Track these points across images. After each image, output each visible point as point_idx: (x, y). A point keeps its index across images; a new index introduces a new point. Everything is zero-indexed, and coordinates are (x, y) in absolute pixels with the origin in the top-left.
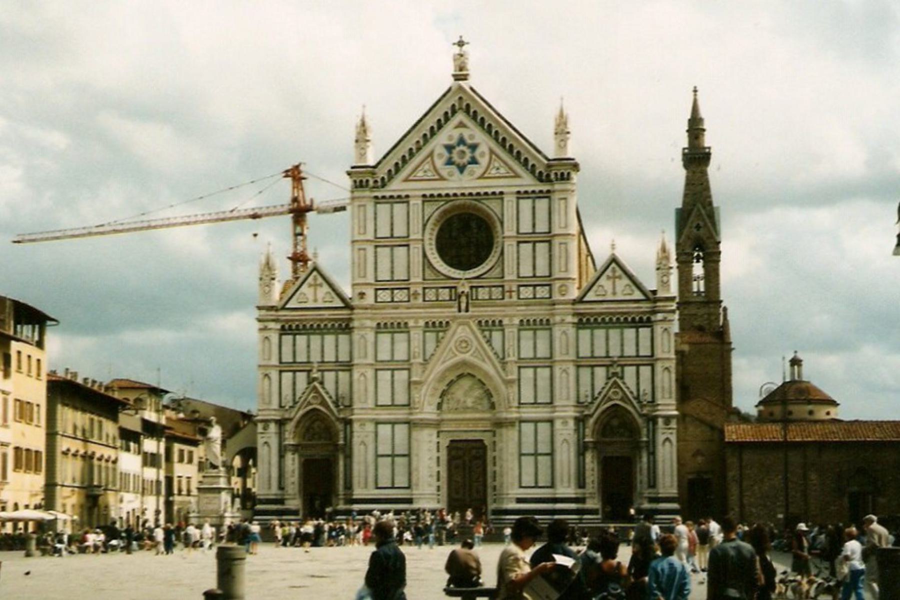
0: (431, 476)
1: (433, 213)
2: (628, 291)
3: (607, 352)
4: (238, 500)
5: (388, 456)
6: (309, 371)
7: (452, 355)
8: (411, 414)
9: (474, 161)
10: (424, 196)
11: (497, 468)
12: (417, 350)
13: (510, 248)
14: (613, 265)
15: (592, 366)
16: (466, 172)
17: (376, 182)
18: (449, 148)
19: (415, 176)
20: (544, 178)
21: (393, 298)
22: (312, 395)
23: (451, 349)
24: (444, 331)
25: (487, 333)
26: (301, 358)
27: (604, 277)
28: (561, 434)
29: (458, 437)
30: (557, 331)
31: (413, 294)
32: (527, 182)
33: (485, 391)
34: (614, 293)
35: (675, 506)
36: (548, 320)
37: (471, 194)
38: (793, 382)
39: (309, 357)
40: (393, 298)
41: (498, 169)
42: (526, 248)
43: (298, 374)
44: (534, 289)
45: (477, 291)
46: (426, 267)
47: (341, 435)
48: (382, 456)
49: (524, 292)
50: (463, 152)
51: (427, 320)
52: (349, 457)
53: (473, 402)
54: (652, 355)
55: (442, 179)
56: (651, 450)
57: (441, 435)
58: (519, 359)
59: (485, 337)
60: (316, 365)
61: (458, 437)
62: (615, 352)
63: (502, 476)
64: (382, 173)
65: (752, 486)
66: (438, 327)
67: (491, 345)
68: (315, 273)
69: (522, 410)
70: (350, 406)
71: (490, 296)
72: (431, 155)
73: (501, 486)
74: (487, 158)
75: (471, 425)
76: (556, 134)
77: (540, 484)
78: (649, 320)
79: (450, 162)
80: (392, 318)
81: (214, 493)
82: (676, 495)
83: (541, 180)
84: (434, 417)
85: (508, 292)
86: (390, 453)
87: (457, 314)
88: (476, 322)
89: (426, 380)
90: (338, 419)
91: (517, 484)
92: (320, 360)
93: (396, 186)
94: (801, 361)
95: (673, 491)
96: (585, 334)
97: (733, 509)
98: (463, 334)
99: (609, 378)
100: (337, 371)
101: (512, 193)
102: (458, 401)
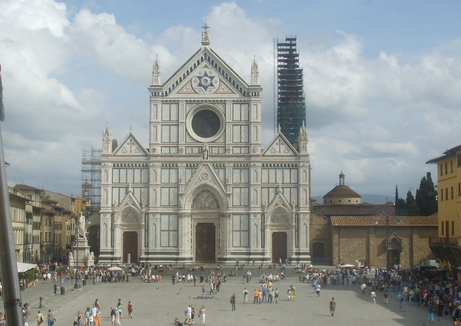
0: (188, 241)
1: (191, 109)
2: (286, 151)
3: (276, 181)
4: (93, 253)
6: (127, 188)
8: (179, 210)
10: (187, 101)
11: (221, 238)
12: (182, 178)
13: (229, 128)
15: (269, 188)
16: (208, 89)
17: (163, 93)
18: (200, 78)
20: (246, 94)
21: (170, 152)
24: (196, 169)
25: (217, 170)
26: (123, 180)
27: (275, 143)
30: (252, 171)
31: (180, 150)
32: (237, 96)
33: (215, 199)
34: (280, 152)
35: (308, 256)
36: (247, 164)
37: (210, 101)
38: (340, 185)
39: (127, 180)
40: (170, 152)
41: (223, 89)
42: (237, 128)
43: (121, 189)
44: (241, 149)
45: (212, 149)
46: (187, 135)
47: (143, 220)
49: (235, 150)
50: (206, 80)
51: (187, 163)
52: (147, 231)
53: (209, 205)
54: (298, 183)
55: (196, 93)
57: (192, 220)
58: (233, 183)
59: (216, 172)
60: (130, 184)
62: (279, 181)
63: (223, 241)
64: (166, 89)
65: (344, 247)
66: (192, 167)
68: (131, 138)
70: (148, 206)
71: (219, 152)
72: (191, 81)
73: (223, 245)
74: (218, 83)
75: (208, 216)
76: (252, 73)
78: (296, 165)
79: (200, 85)
81: (82, 250)
82: (309, 251)
83: (244, 95)
84: (190, 211)
85: (227, 150)
86: (168, 229)
87: (203, 160)
88: (212, 164)
89: (187, 193)
90: (142, 212)
91: (231, 246)
92: (133, 182)
93: (173, 96)
94: (344, 176)
95: (307, 250)
96: (265, 172)
97: (335, 258)
99: (276, 194)
102: (202, 204)
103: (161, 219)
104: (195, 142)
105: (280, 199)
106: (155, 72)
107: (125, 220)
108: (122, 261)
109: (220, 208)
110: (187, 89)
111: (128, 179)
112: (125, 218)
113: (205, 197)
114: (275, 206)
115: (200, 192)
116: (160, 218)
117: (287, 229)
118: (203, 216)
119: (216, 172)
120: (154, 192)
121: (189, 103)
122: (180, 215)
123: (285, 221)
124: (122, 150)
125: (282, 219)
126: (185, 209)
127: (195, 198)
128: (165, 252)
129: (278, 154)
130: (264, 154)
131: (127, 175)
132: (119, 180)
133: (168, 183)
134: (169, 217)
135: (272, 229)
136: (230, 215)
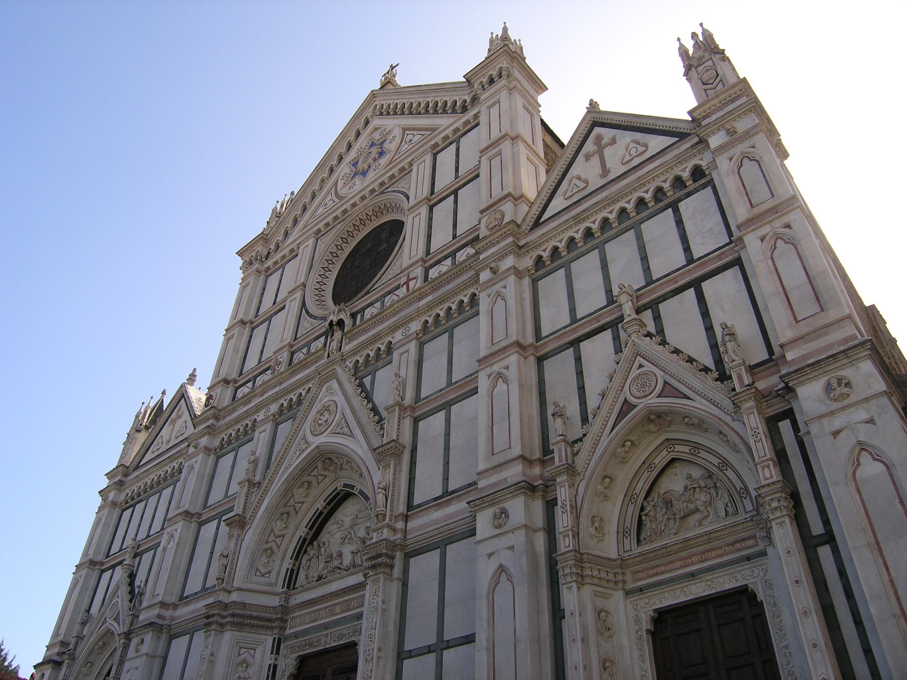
9: (381, 154)
10: (319, 231)
23: (304, 438)
27: (581, 157)
28: (490, 555)
32: (446, 123)
34: (605, 171)
56: (817, 528)
59: (361, 385)
67: (369, 398)
69: (411, 525)
72: (336, 184)
74: (398, 139)
75: (338, 609)
84: (275, 601)
88: (351, 365)
98: (327, 399)
103: (165, 659)
105: (641, 366)
114: (621, 415)
116: (160, 651)
117: (748, 558)
119: (361, 385)
125: (703, 497)
126: (236, 584)
127: (301, 537)
130: (540, 217)
135: (641, 590)
136: (393, 558)
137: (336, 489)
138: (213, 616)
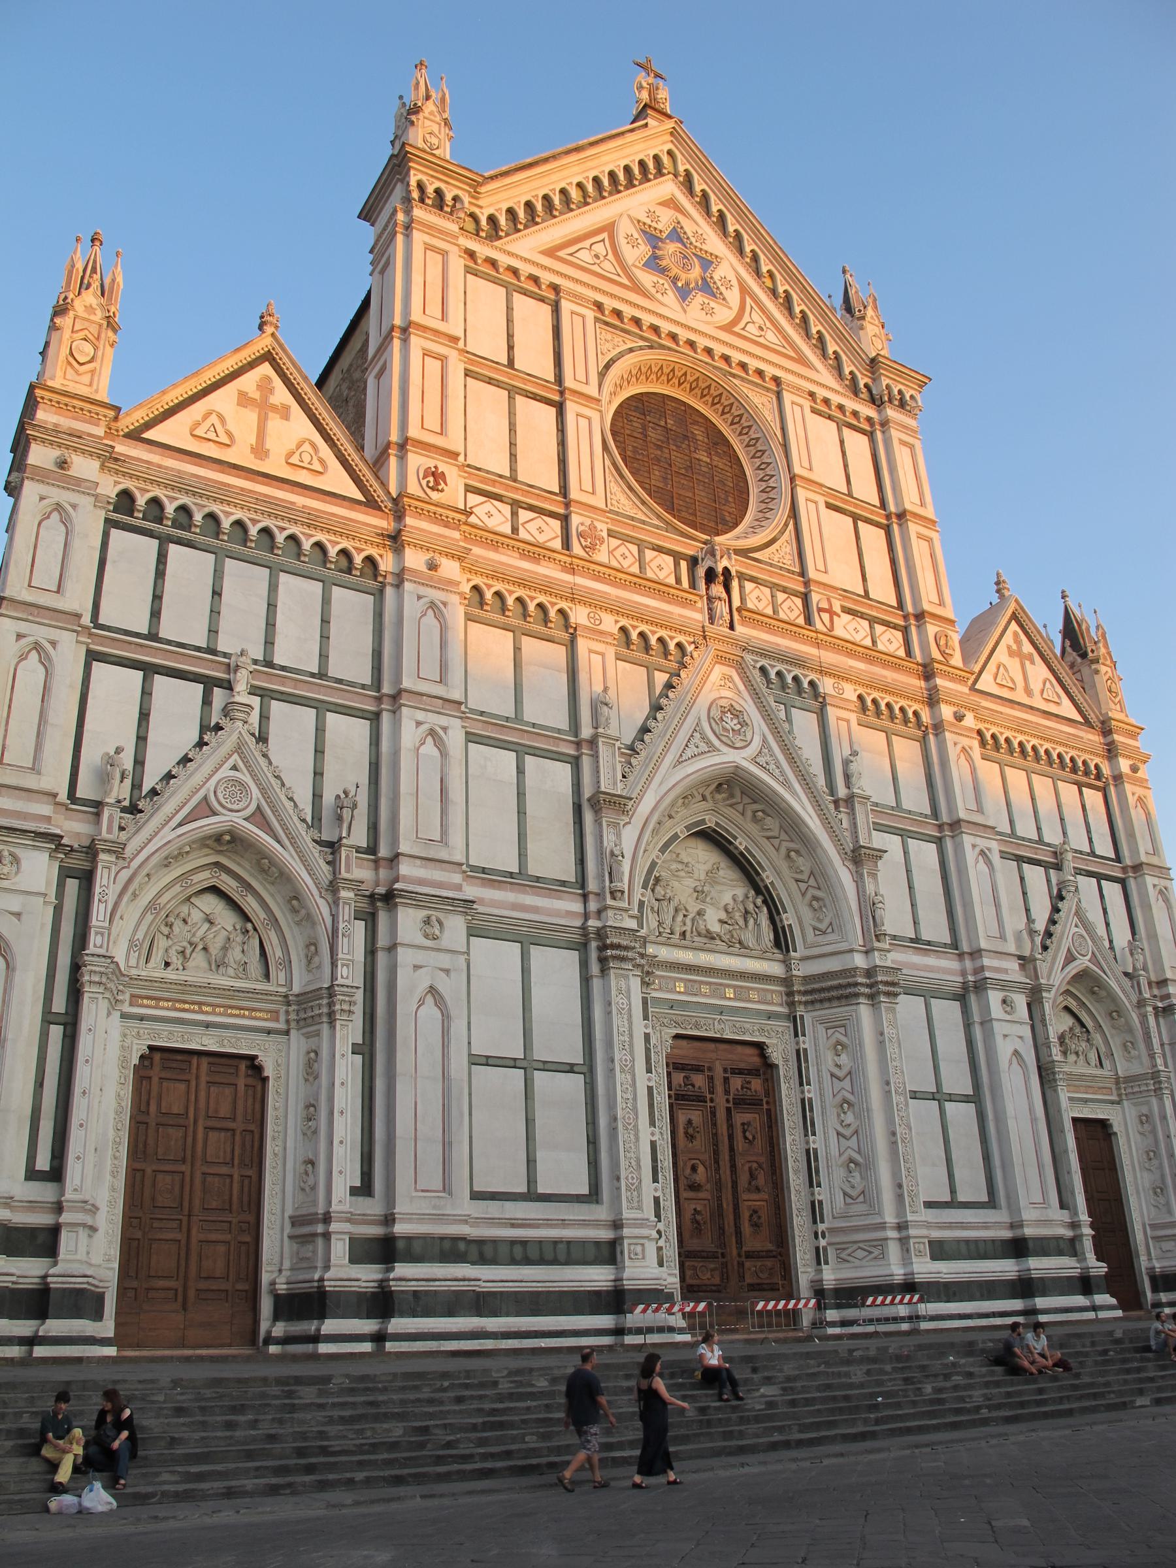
5: (513, 1063)
7: (703, 747)
10: (599, 306)
14: (1014, 626)
19: (571, 255)
22: (225, 772)
29: (697, 1026)
39: (213, 631)
41: (761, 328)
48: (488, 1061)
53: (721, 921)
55: (637, 288)
61: (697, 1026)
63: (860, 1164)
77: (962, 1197)
79: (654, 263)
80: (522, 583)
98: (726, 693)
100: (322, 708)
101: (798, 390)
104: (656, 522)
106: (427, 115)
107: (162, 943)
108: (107, 1327)
109: (795, 951)
110: (597, 256)
111: (224, 625)
112: (166, 930)
113: (701, 871)
115: (680, 829)
118: (705, 989)
120: (429, 749)
121: (607, 324)
122: (618, 947)
123: (1093, 1056)
124: (197, 424)
128: (513, 1242)
129: (1026, 700)
131: (217, 593)
132: (155, 614)
133: (507, 719)
134: (525, 957)
137: (703, 822)
138: (626, 948)
